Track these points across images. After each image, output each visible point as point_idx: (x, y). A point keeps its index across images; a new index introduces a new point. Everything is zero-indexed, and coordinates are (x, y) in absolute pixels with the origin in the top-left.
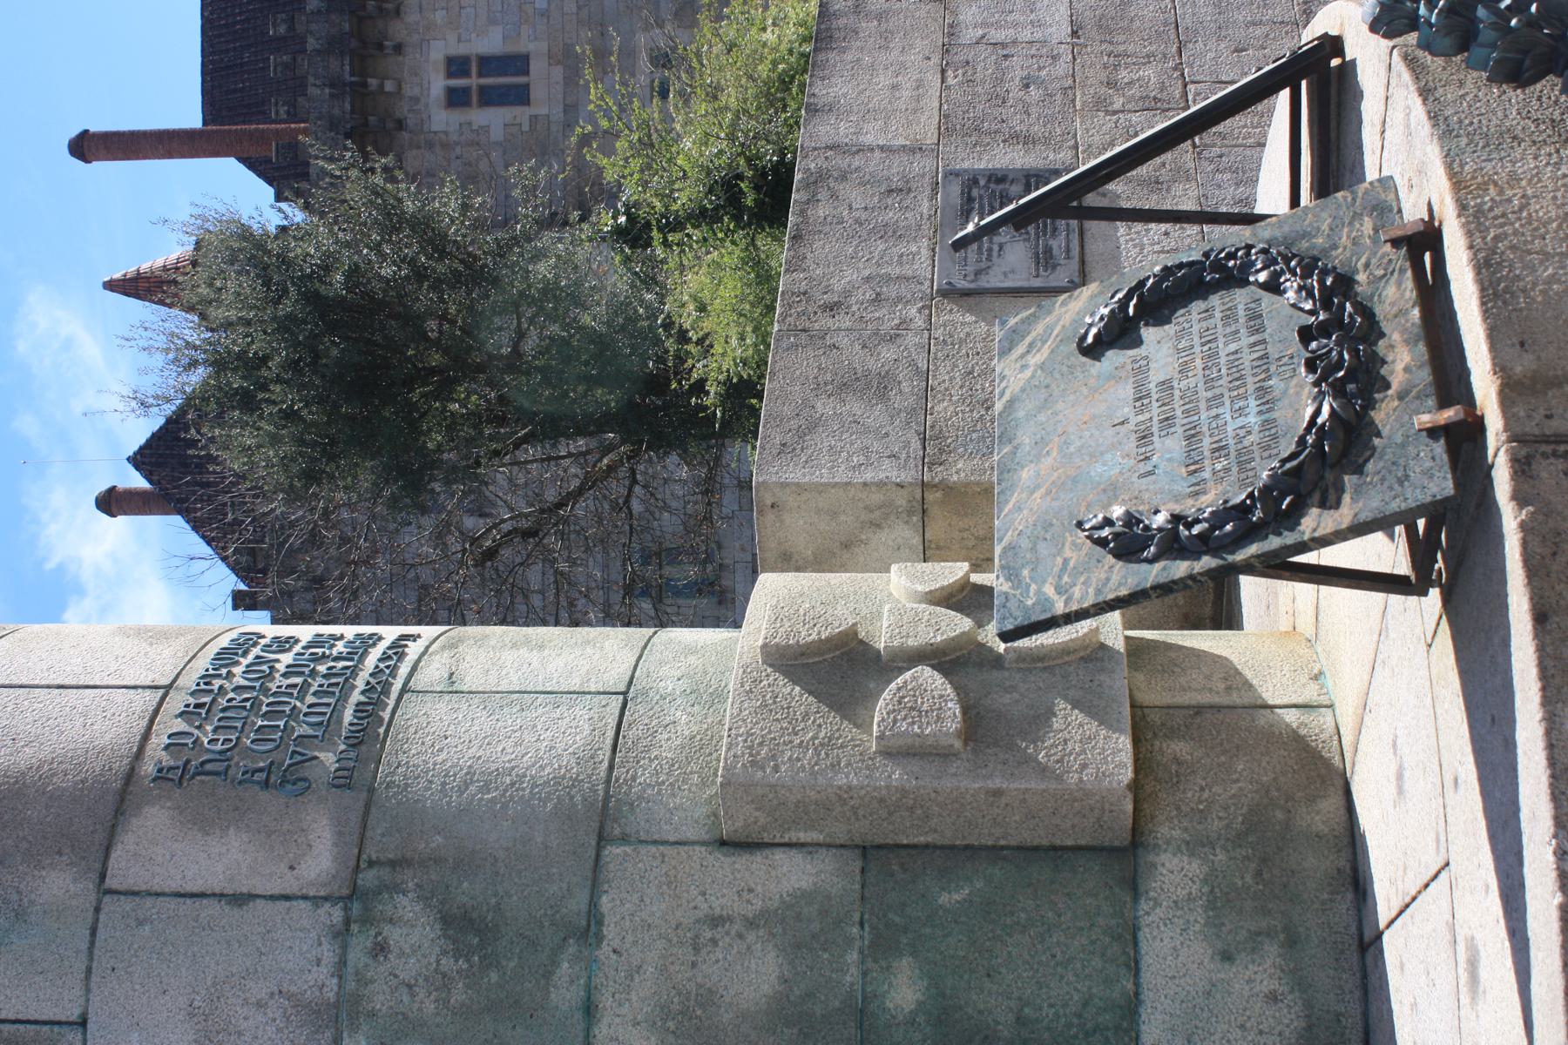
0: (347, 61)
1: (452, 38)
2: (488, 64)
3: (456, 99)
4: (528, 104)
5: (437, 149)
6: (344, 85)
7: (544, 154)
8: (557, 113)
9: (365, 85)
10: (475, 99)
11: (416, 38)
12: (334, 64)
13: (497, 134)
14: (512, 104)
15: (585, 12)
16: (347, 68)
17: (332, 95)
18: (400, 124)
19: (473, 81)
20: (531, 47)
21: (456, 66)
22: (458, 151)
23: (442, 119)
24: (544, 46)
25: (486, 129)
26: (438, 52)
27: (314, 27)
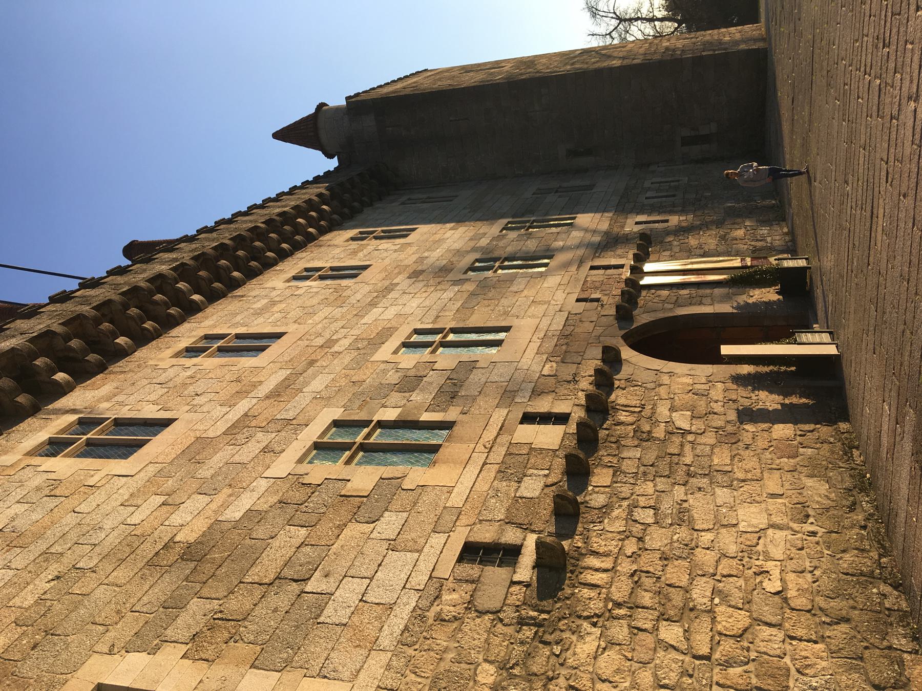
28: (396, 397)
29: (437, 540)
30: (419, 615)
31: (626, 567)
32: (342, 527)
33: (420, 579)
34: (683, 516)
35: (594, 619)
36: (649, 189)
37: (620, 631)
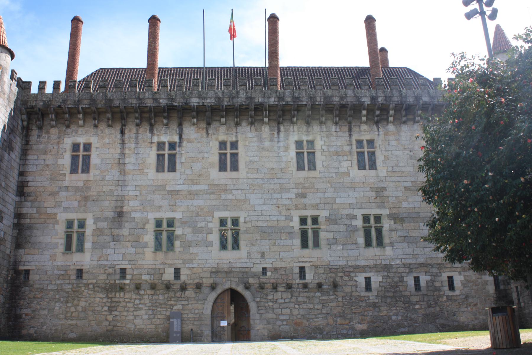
0: (87, 106)
1: (98, 145)
2: (87, 159)
3: (76, 147)
4: (71, 173)
5: (58, 140)
6: (78, 105)
7: (51, 179)
8: (66, 184)
9: (79, 113)
10: (74, 153)
11: (99, 132)
12: (86, 102)
13: (60, 162)
14: (71, 167)
15: (102, 194)
16: (84, 106)
17: (75, 101)
18: (68, 127)
19: (81, 153)
20: (91, 174)
21: (88, 147)
22: (56, 147)
23: (68, 142)
24: (91, 179)
25: (63, 158)
26: (93, 140)
27: (101, 94)
28: (188, 230)
29: (127, 262)
30: (106, 266)
31: (121, 300)
32: (129, 241)
33: (115, 263)
34: (137, 309)
35: (107, 296)
36: (435, 276)
37: (105, 300)
